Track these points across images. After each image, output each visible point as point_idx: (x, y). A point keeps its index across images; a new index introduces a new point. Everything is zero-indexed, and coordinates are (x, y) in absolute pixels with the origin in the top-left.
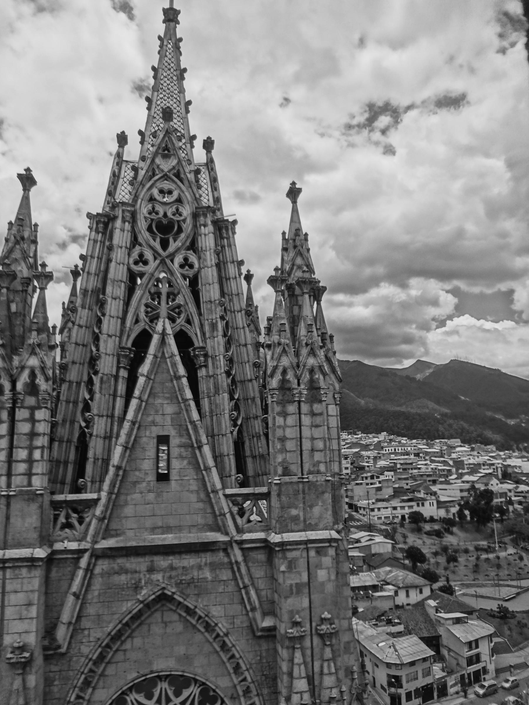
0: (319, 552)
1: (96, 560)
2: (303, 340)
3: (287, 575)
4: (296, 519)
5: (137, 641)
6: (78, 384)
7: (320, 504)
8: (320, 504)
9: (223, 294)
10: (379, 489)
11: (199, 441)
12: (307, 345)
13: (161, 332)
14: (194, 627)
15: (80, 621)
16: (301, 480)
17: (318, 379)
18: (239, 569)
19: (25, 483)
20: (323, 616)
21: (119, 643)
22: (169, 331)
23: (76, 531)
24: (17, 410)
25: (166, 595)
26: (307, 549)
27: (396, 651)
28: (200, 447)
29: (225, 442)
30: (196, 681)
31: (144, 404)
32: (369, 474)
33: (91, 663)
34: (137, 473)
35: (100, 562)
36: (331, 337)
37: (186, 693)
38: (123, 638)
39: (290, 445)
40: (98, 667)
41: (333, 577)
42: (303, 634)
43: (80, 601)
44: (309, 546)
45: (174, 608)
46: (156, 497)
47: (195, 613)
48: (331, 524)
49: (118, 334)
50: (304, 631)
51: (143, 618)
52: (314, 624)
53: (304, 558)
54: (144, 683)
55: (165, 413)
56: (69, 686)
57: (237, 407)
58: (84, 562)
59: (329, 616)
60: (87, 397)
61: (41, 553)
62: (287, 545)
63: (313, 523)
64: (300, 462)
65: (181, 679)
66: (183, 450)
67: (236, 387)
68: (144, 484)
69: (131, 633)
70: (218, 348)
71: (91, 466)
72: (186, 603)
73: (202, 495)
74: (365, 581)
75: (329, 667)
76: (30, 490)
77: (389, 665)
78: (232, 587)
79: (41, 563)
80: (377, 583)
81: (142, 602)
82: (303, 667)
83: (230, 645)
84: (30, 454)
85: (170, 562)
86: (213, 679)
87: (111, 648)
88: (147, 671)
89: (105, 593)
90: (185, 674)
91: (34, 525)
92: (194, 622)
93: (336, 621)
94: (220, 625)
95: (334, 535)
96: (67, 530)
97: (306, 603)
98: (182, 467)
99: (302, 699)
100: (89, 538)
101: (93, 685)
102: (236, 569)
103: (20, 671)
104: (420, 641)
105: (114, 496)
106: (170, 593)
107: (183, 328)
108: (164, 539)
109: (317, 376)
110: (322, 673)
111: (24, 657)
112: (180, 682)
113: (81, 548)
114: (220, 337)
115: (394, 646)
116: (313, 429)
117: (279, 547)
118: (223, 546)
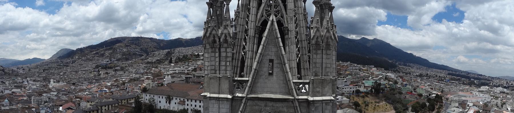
0: (326, 104)
4: (318, 92)
9: (295, 7)
11: (284, 62)
28: (285, 64)
35: (249, 101)
57: (299, 50)
61: (230, 97)
73: (285, 82)
84: (226, 63)
95: (332, 98)
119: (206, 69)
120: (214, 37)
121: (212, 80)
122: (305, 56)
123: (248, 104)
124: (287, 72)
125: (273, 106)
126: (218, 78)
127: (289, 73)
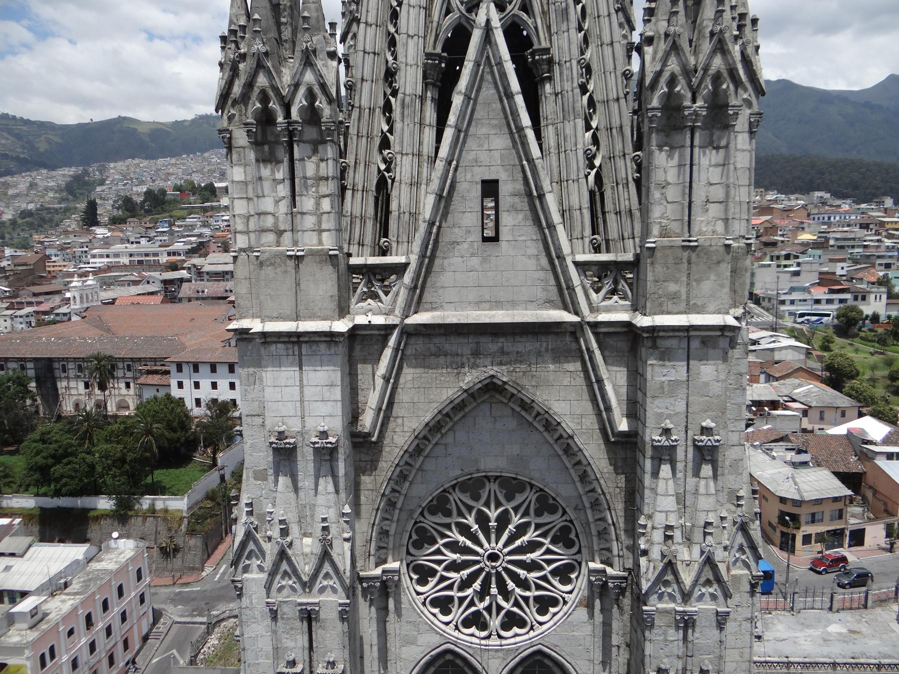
0: (705, 342)
1: (407, 338)
2: (707, 26)
3: (657, 369)
4: (674, 297)
5: (461, 435)
6: (372, 110)
7: (713, 277)
8: (713, 277)
10: (797, 274)
11: (539, 187)
12: (712, 34)
13: (483, 24)
14: (530, 424)
15: (392, 408)
16: (687, 244)
17: (726, 91)
18: (591, 358)
19: (315, 241)
20: (704, 424)
21: (439, 436)
22: (496, 23)
23: (381, 301)
24: (295, 146)
25: (495, 384)
26: (689, 338)
27: (796, 484)
28: (541, 197)
29: (576, 189)
30: (532, 486)
31: (462, 134)
32: (784, 253)
33: (407, 455)
34: (456, 230)
35: (412, 341)
36: (755, 21)
37: (519, 499)
38: (443, 431)
39: (673, 193)
40: (415, 461)
41: (722, 377)
42: (675, 443)
43: (390, 385)
44: (692, 333)
45: (505, 401)
46: (481, 263)
47: (532, 407)
48: (727, 306)
49: (421, 33)
50: (676, 441)
51: (467, 410)
52: (690, 433)
53: (683, 349)
54: (470, 482)
55: (491, 148)
56: (382, 478)
57: (595, 140)
58: (392, 341)
59: (713, 425)
60: (386, 128)
61: (342, 326)
62: (659, 331)
63: (699, 303)
64: (686, 218)
65: (514, 482)
66: (517, 199)
67: (594, 111)
68: (466, 246)
69: (453, 426)
70: (570, 50)
71: (396, 222)
72: (520, 395)
73: (544, 262)
74: (760, 395)
75: (707, 486)
76: (322, 250)
77: (783, 500)
78: (580, 380)
79: (342, 339)
80: (777, 398)
81: (466, 391)
82: (671, 482)
83: (576, 449)
84: (318, 204)
85: (500, 345)
86: (554, 486)
87: (429, 441)
88: (472, 470)
89: (421, 377)
90: (519, 477)
91: (331, 294)
92: (530, 419)
93: (721, 432)
94: (563, 425)
95: (731, 321)
96: (369, 301)
97: (681, 407)
98: (516, 222)
99: (667, 520)
100: (397, 312)
101: (410, 479)
102: (587, 357)
103: (328, 458)
104: (833, 476)
105: (427, 260)
106: (500, 383)
107: (515, 19)
108: (493, 316)
109: (724, 86)
110: (696, 492)
111: (330, 443)
112: (512, 486)
113: (388, 323)
114: (573, 31)
115: (793, 478)
116: (711, 169)
117: (647, 332)
118: (572, 329)
119: (240, 227)
120: (264, 98)
121: (269, 271)
122: (620, 163)
123: (409, 352)
124: (551, 227)
125: (503, 352)
126: (291, 263)
127: (561, 231)
